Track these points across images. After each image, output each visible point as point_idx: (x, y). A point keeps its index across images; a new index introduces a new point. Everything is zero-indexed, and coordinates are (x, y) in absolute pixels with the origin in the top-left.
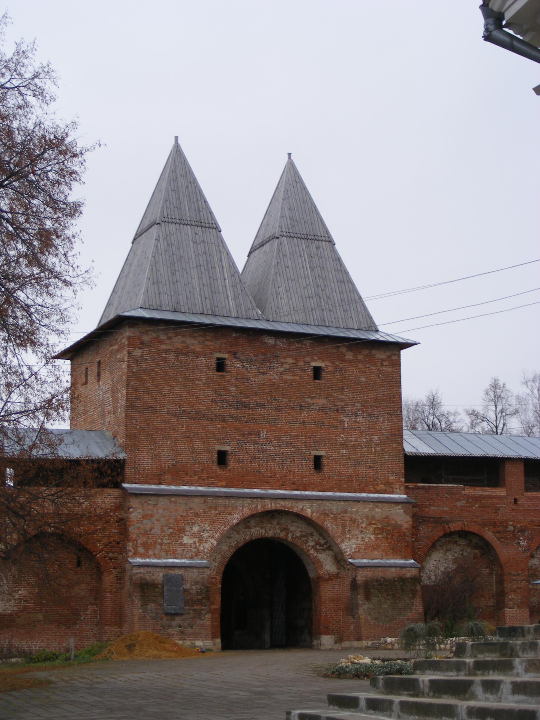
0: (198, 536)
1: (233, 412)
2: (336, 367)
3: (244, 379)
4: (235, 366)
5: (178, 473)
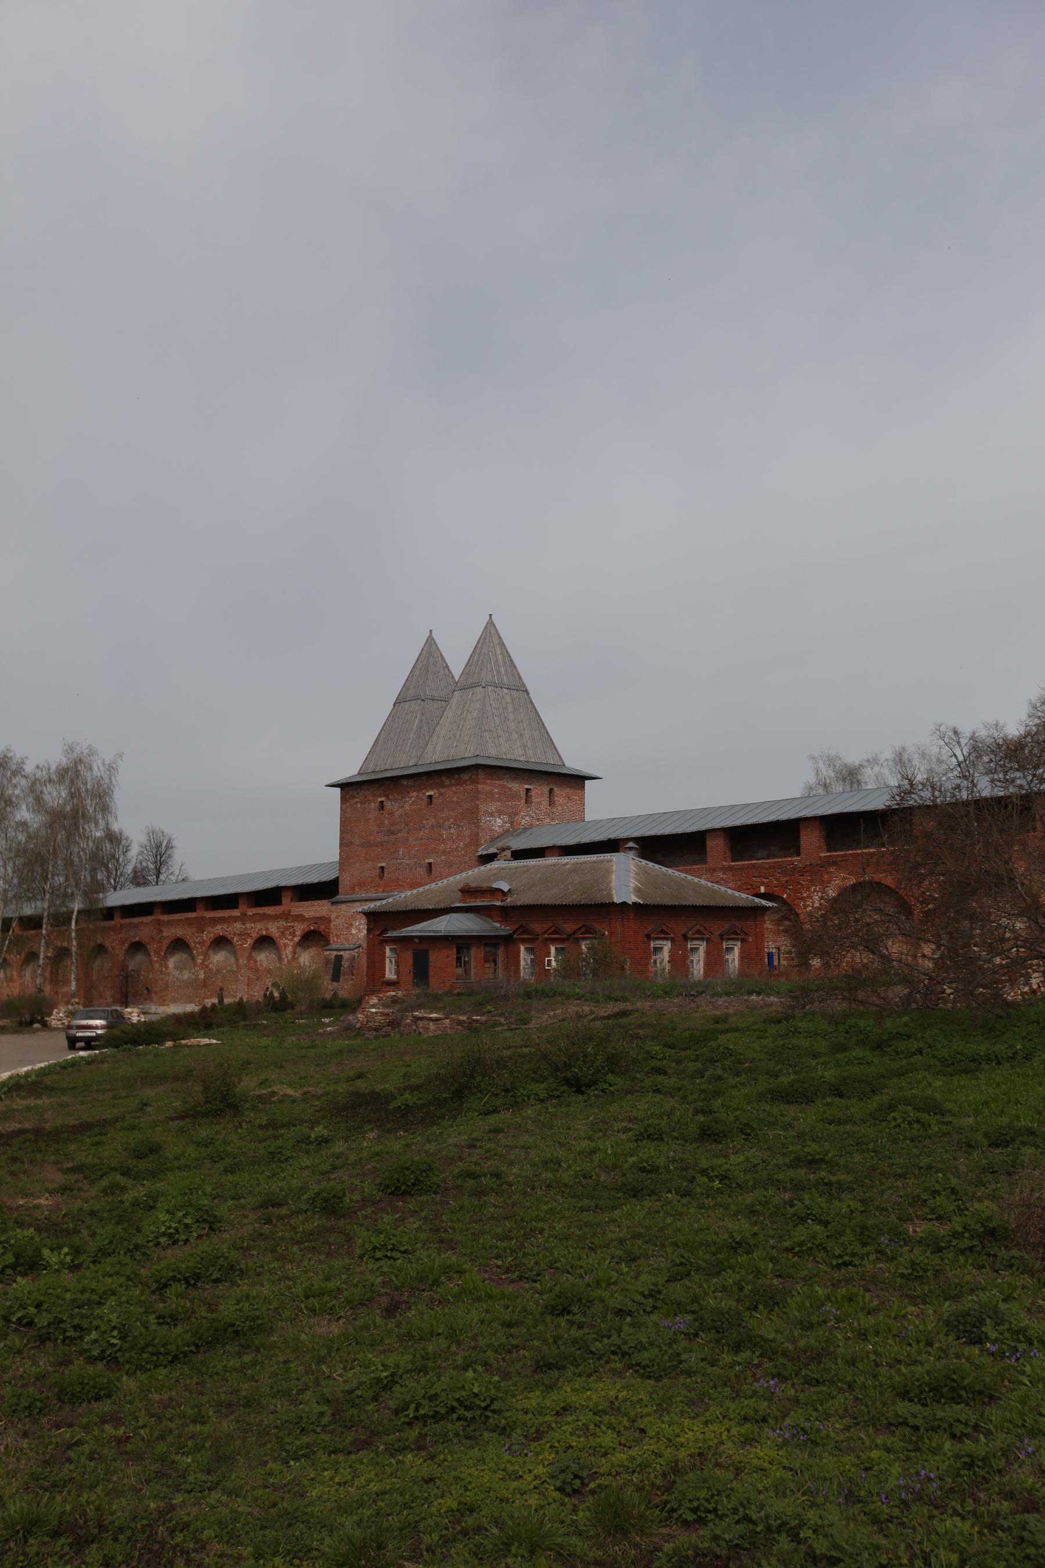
0: (357, 928)
1: (386, 838)
2: (441, 794)
3: (392, 814)
4: (388, 804)
5: (361, 884)
